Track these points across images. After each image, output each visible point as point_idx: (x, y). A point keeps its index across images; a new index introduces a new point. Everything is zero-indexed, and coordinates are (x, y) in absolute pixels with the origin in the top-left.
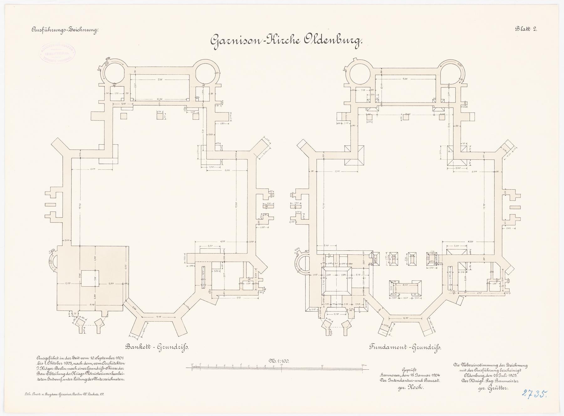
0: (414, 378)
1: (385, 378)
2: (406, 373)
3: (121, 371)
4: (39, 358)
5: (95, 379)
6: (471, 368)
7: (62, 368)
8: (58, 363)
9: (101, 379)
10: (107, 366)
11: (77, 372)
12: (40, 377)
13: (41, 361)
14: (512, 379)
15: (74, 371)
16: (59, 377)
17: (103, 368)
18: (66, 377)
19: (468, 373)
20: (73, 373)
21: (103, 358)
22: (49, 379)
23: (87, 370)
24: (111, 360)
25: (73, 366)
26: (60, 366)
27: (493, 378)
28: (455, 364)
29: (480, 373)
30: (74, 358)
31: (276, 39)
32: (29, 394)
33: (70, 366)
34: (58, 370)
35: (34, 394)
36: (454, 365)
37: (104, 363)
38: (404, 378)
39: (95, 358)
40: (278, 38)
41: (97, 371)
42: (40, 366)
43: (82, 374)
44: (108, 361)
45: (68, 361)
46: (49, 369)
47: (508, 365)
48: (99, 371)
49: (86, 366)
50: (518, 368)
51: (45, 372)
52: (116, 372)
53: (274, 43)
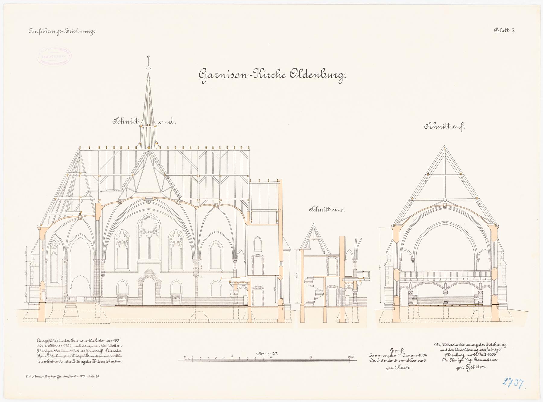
0: (402, 358)
1: (375, 358)
2: (394, 354)
5: (94, 361)
6: (452, 348)
7: (61, 351)
8: (57, 346)
9: (99, 362)
10: (105, 349)
11: (75, 355)
12: (40, 359)
14: (491, 357)
15: (73, 353)
16: (58, 359)
17: (102, 351)
18: (66, 359)
19: (448, 352)
21: (101, 341)
22: (49, 362)
23: (86, 353)
24: (109, 343)
25: (72, 349)
26: (59, 349)
27: (472, 358)
28: (437, 345)
29: (460, 353)
30: (73, 340)
31: (262, 73)
32: (30, 377)
33: (69, 349)
35: (35, 376)
36: (435, 344)
37: (103, 346)
38: (391, 358)
40: (265, 73)
41: (95, 354)
42: (40, 348)
43: (80, 356)
44: (106, 344)
47: (487, 345)
48: (98, 354)
49: (85, 349)
50: (497, 347)
51: (46, 354)
52: (115, 354)
53: (261, 78)
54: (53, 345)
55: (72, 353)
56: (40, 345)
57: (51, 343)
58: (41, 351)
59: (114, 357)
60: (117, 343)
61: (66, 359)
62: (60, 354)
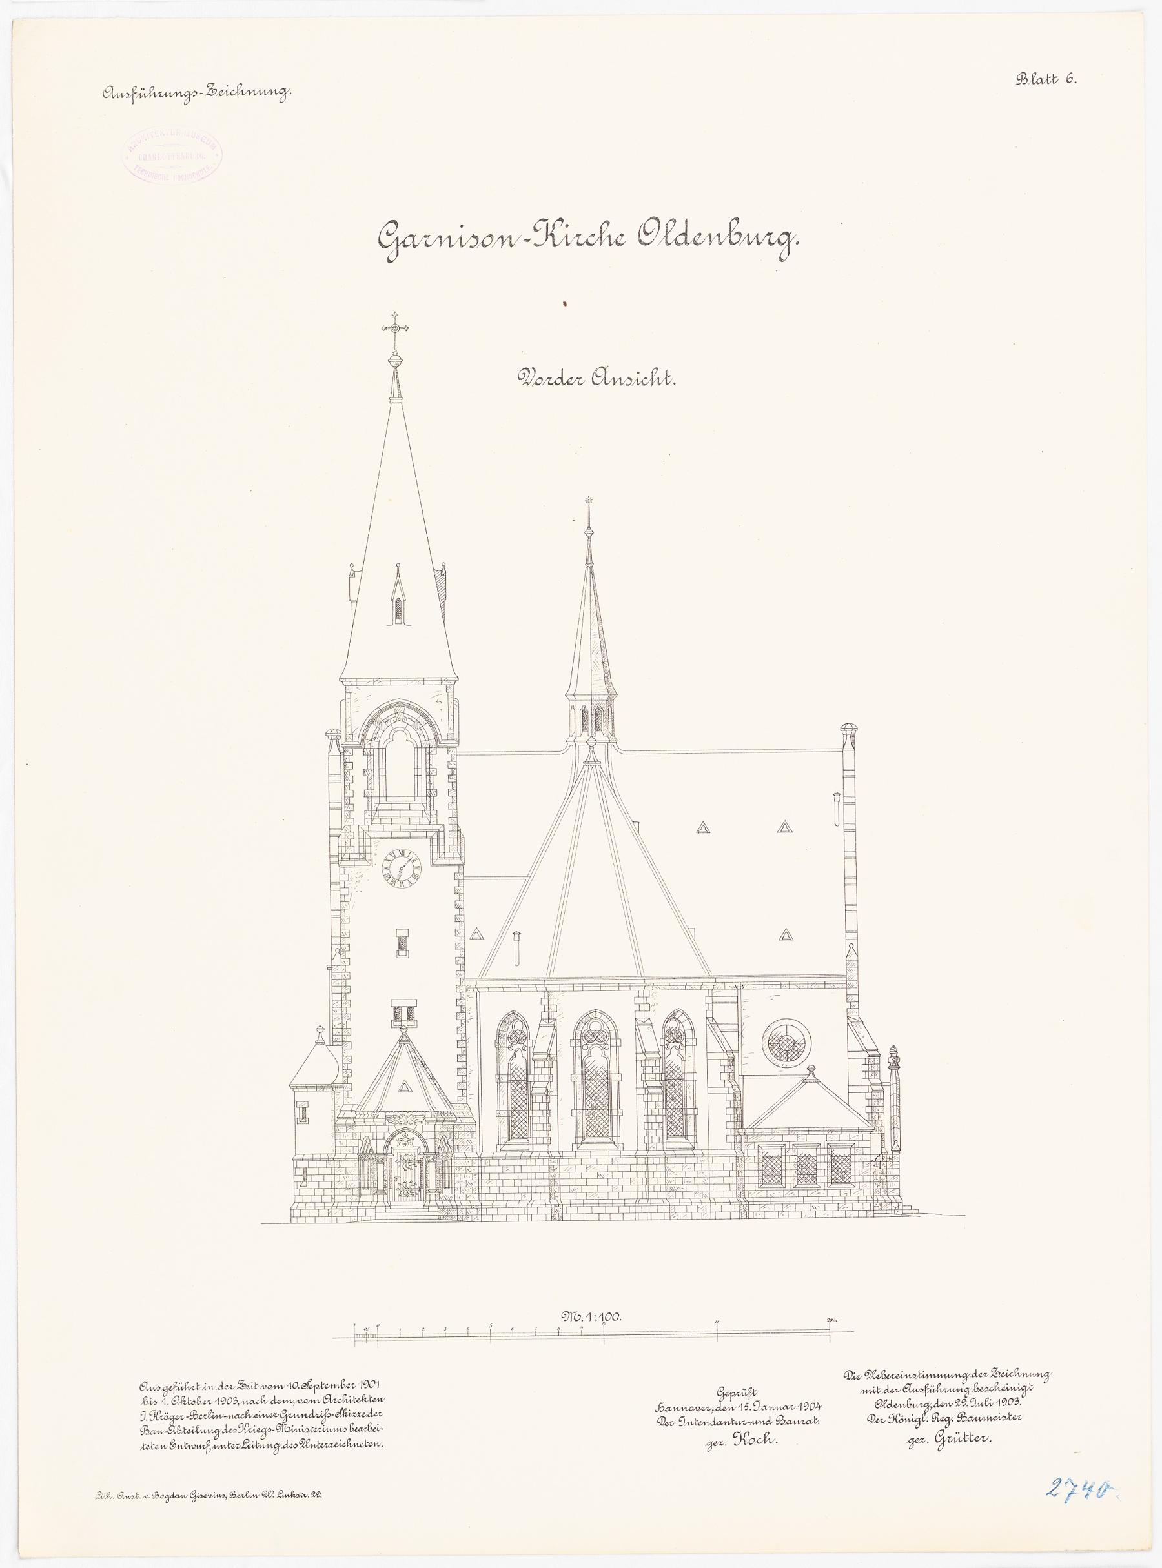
3: (375, 1421)
4: (144, 1386)
5: (304, 1443)
7: (210, 1416)
9: (320, 1446)
10: (334, 1408)
12: (148, 1440)
13: (150, 1394)
15: (245, 1421)
16: (201, 1439)
17: (326, 1415)
18: (224, 1439)
20: (241, 1428)
22: (173, 1445)
24: (345, 1390)
25: (241, 1410)
30: (242, 1385)
34: (198, 1422)
37: (328, 1399)
39: (300, 1386)
42: (148, 1409)
43: (264, 1431)
45: (227, 1393)
46: (174, 1418)
48: (316, 1423)
49: (277, 1409)
51: (164, 1425)
54: (186, 1399)
55: (241, 1420)
56: (149, 1400)
57: (180, 1393)
58: (152, 1417)
59: (361, 1430)
60: (369, 1392)
61: (224, 1439)
62: (205, 1424)
